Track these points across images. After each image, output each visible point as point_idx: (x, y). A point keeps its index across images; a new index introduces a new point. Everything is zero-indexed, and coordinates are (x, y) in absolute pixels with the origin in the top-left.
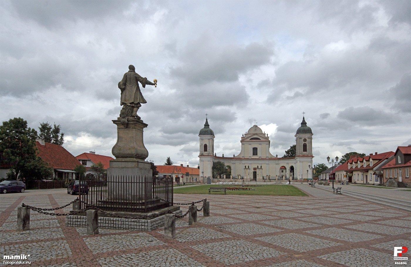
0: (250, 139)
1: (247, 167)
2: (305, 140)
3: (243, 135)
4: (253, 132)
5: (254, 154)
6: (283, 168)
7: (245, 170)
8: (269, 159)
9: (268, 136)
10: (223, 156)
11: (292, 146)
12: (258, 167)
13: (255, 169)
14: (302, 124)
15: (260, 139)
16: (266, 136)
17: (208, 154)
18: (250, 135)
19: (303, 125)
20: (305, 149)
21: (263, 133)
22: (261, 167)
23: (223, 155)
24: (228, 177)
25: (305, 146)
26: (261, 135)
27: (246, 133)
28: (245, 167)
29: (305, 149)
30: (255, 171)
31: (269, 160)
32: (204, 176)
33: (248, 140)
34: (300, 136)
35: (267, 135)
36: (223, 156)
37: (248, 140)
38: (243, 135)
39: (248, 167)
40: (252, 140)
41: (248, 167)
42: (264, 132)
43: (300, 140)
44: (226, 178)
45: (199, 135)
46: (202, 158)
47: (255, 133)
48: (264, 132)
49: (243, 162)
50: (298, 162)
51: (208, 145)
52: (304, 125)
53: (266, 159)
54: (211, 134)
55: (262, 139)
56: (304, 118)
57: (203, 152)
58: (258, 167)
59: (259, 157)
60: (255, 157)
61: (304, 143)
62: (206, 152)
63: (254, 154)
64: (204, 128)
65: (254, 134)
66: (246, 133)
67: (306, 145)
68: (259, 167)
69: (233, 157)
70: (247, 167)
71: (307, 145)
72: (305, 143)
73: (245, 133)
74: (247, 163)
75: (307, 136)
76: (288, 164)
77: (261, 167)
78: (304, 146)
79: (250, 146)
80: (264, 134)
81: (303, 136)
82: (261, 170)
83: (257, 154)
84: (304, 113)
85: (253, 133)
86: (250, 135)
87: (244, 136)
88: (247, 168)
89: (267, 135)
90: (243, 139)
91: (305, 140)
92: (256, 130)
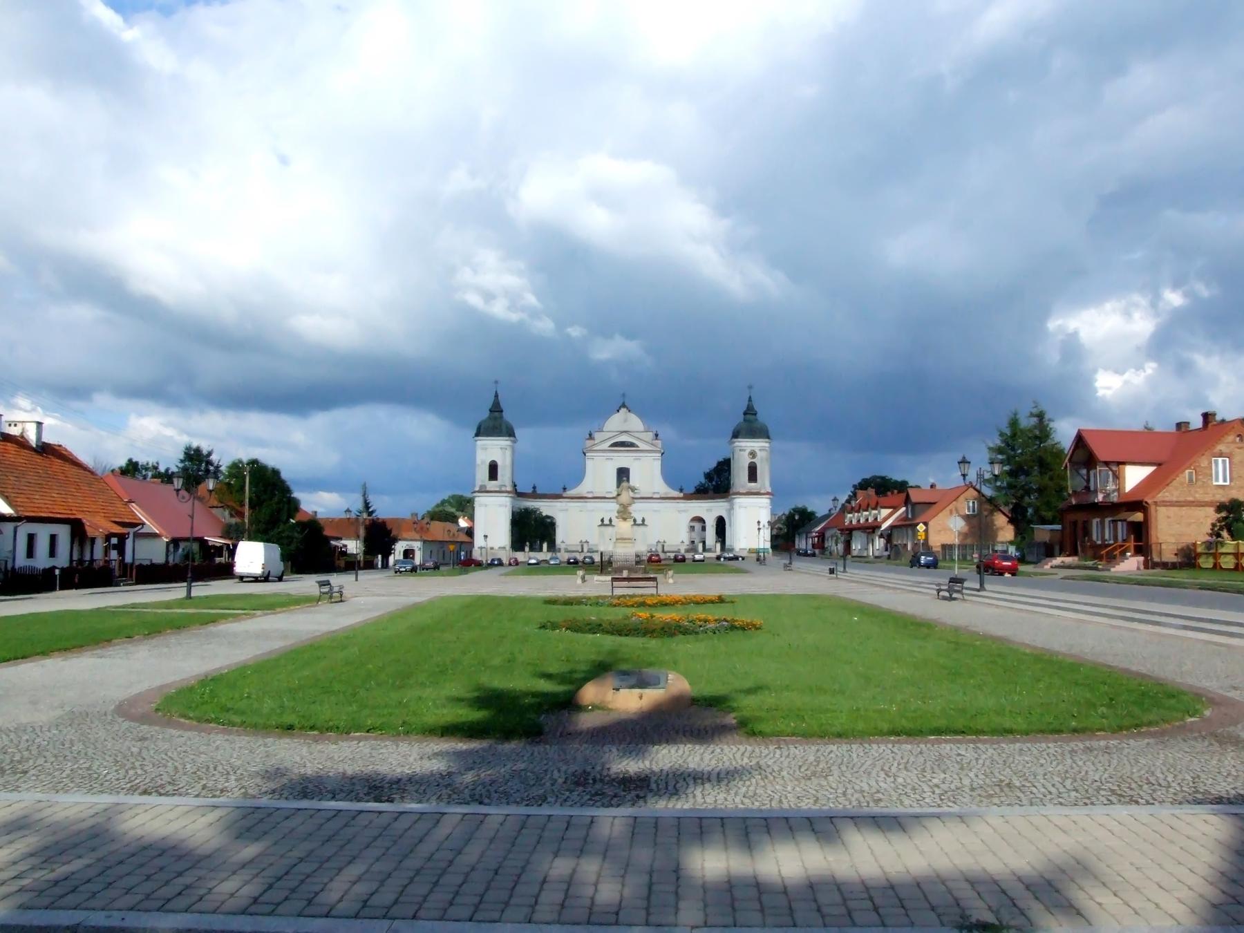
0: (613, 445)
1: (606, 522)
2: (753, 454)
7: (603, 528)
22: (643, 520)
23: (534, 488)
24: (552, 547)
32: (490, 545)
37: (606, 446)
44: (549, 550)
45: (477, 435)
49: (591, 505)
50: (736, 507)
51: (499, 463)
55: (642, 446)
64: (489, 418)
69: (560, 491)
70: (606, 522)
76: (709, 510)
77: (643, 520)
79: (609, 462)
82: (642, 528)
91: (753, 454)
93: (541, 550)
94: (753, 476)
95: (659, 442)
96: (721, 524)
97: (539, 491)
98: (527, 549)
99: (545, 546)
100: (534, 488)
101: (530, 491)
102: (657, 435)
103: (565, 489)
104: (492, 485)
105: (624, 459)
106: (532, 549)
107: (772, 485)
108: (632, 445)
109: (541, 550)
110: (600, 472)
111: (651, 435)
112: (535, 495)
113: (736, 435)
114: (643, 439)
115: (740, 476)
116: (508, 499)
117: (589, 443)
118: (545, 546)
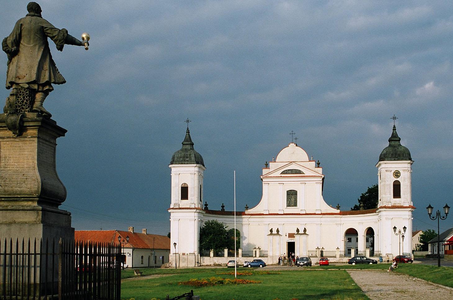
0: (282, 173)
1: (275, 232)
2: (397, 174)
5: (289, 205)
6: (351, 233)
7: (271, 237)
8: (322, 214)
9: (319, 166)
10: (223, 210)
11: (370, 188)
12: (298, 230)
13: (291, 235)
14: (390, 140)
19: (393, 143)
22: (305, 230)
23: (223, 207)
28: (271, 231)
31: (321, 216)
36: (223, 210)
37: (278, 174)
39: (278, 231)
41: (278, 231)
43: (388, 173)
52: (397, 143)
53: (315, 214)
54: (197, 163)
55: (307, 173)
56: (394, 129)
58: (298, 230)
59: (301, 210)
60: (292, 210)
61: (396, 179)
63: (289, 205)
67: (400, 185)
68: (301, 231)
70: (275, 232)
72: (398, 179)
74: (275, 223)
77: (305, 230)
78: (394, 185)
83: (295, 205)
85: (288, 161)
88: (275, 235)
91: (397, 174)
93: (223, 255)
94: (397, 193)
95: (320, 170)
96: (370, 232)
97: (226, 210)
98: (212, 254)
99: (226, 251)
100: (223, 207)
101: (220, 209)
102: (319, 164)
103: (247, 208)
104: (184, 203)
105: (292, 184)
106: (216, 255)
107: (413, 199)
108: (299, 172)
109: (223, 255)
110: (273, 194)
111: (313, 163)
112: (223, 212)
113: (383, 158)
114: (310, 168)
115: (385, 195)
116: (196, 214)
117: (265, 171)
118: (226, 251)
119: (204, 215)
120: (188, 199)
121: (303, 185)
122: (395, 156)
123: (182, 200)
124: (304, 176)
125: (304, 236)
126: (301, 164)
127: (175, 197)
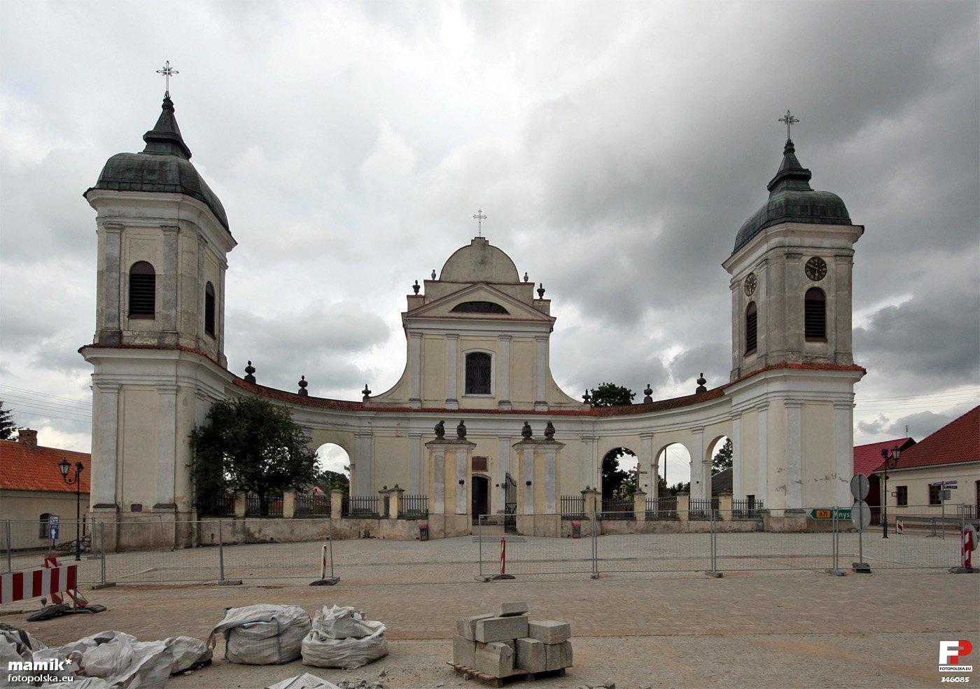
0: (456, 309)
3: (416, 288)
4: (466, 272)
9: (544, 298)
15: (501, 310)
16: (536, 296)
17: (163, 334)
18: (456, 287)
20: (816, 325)
21: (522, 280)
25: (815, 308)
26: (509, 290)
27: (434, 276)
29: (816, 325)
30: (481, 473)
33: (445, 310)
34: (788, 240)
35: (541, 292)
37: (445, 310)
38: (416, 288)
40: (465, 315)
42: (526, 278)
46: (107, 368)
47: (482, 279)
48: (526, 278)
55: (515, 311)
57: (124, 317)
62: (144, 324)
65: (474, 283)
66: (434, 276)
71: (830, 298)
73: (431, 279)
75: (827, 243)
78: (808, 302)
80: (526, 284)
81: (808, 241)
84: (789, 120)
85: (469, 280)
86: (451, 288)
87: (422, 292)
89: (541, 292)
90: (416, 304)
92: (483, 262)
105: (479, 336)
119: (226, 390)
120: (157, 315)
121: (505, 344)
122: (812, 211)
123: (131, 321)
124: (508, 319)
125: (549, 452)
126: (502, 288)
127: (106, 307)
